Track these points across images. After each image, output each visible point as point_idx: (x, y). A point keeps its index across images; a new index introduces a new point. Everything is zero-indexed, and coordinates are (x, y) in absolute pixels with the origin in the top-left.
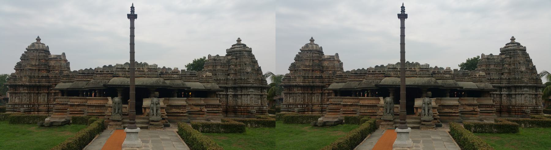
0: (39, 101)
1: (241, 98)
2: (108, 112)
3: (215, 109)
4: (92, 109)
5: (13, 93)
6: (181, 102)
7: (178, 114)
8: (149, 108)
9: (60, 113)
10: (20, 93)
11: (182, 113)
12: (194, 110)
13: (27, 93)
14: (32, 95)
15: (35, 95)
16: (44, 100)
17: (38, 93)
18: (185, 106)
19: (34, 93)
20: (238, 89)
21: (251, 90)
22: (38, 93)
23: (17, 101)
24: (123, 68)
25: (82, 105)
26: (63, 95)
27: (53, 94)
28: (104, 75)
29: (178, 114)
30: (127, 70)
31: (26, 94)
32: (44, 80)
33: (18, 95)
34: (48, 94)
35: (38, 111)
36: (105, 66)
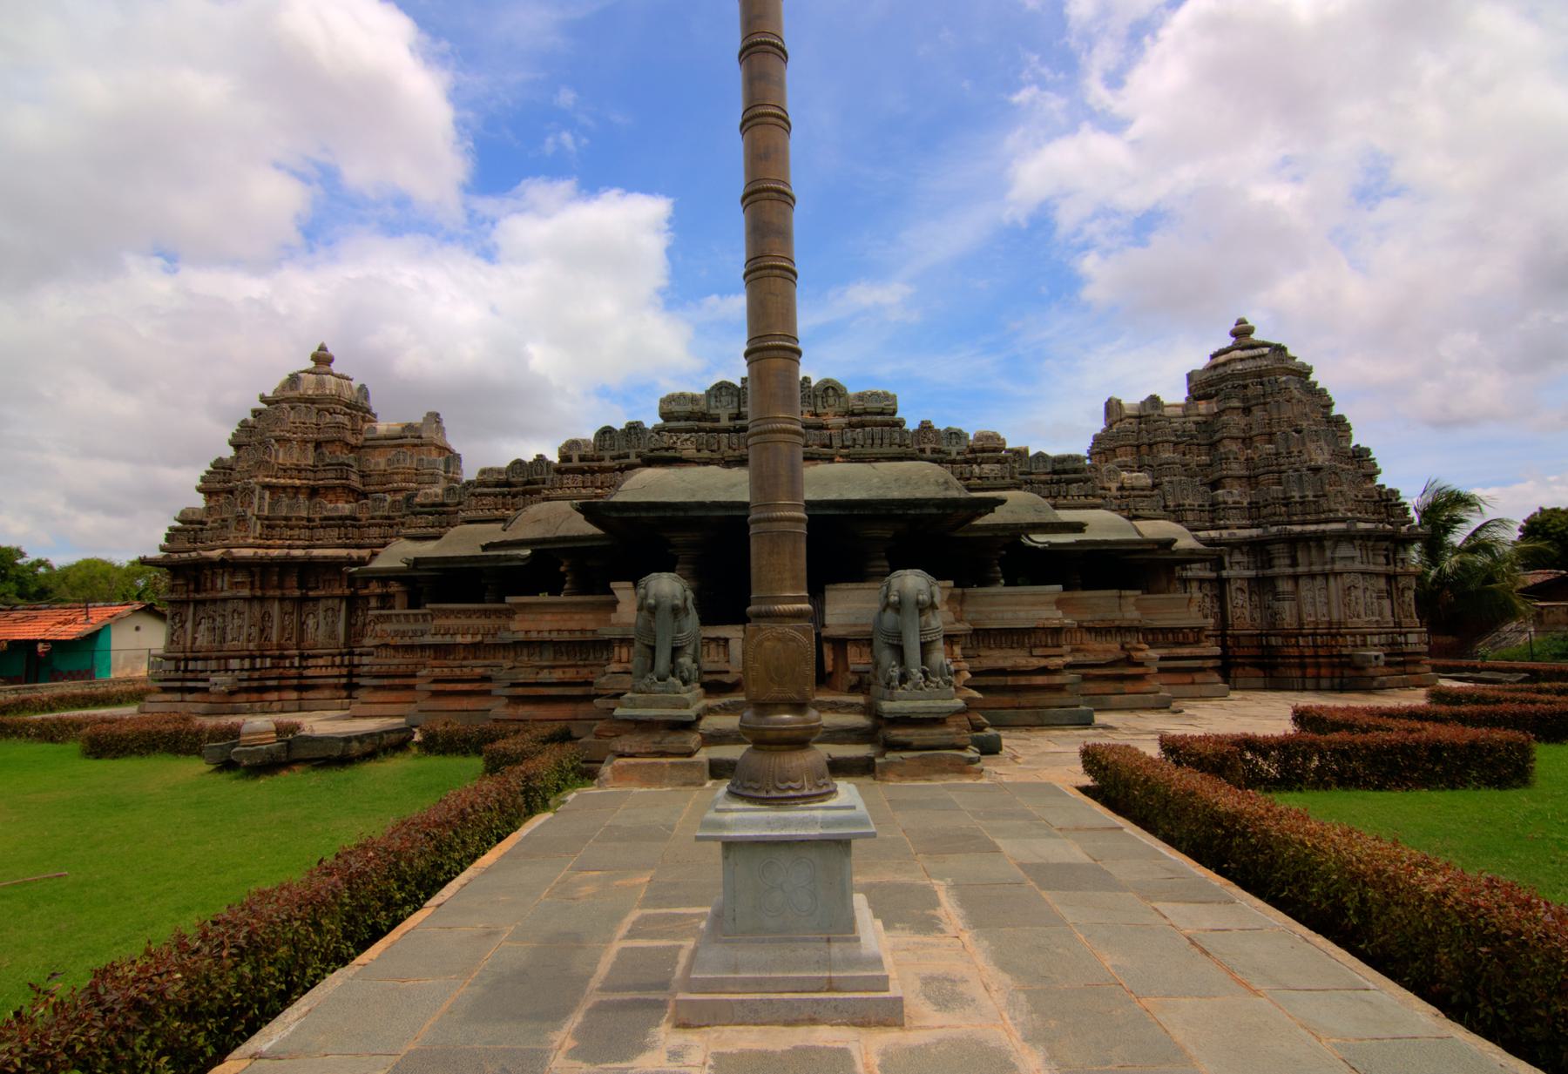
0: (309, 641)
1: (1294, 596)
2: (613, 671)
3: (1185, 651)
4: (536, 661)
5: (186, 603)
6: (1036, 605)
7: (1023, 681)
8: (866, 641)
9: (392, 696)
10: (214, 601)
11: (1044, 671)
12: (1091, 659)
13: (245, 599)
14: (275, 609)
15: (288, 607)
16: (332, 635)
17: (303, 600)
18: (1057, 631)
19: (282, 599)
20: (1278, 550)
21: (1344, 550)
22: (303, 600)
23: (203, 640)
24: (704, 417)
25: (495, 645)
26: (414, 603)
27: (373, 603)
28: (599, 477)
29: (1023, 681)
30: (725, 422)
31: (241, 606)
32: (335, 533)
33: (210, 608)
34: (354, 603)
35: (300, 688)
36: (606, 432)
